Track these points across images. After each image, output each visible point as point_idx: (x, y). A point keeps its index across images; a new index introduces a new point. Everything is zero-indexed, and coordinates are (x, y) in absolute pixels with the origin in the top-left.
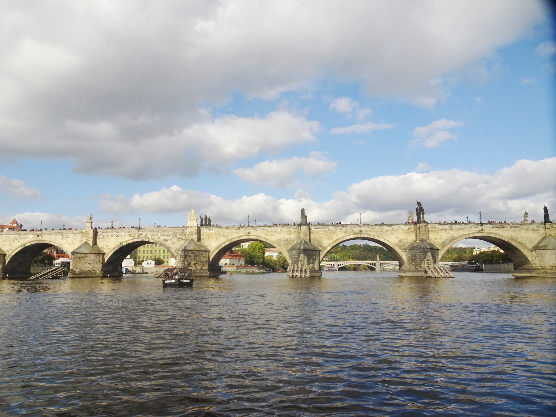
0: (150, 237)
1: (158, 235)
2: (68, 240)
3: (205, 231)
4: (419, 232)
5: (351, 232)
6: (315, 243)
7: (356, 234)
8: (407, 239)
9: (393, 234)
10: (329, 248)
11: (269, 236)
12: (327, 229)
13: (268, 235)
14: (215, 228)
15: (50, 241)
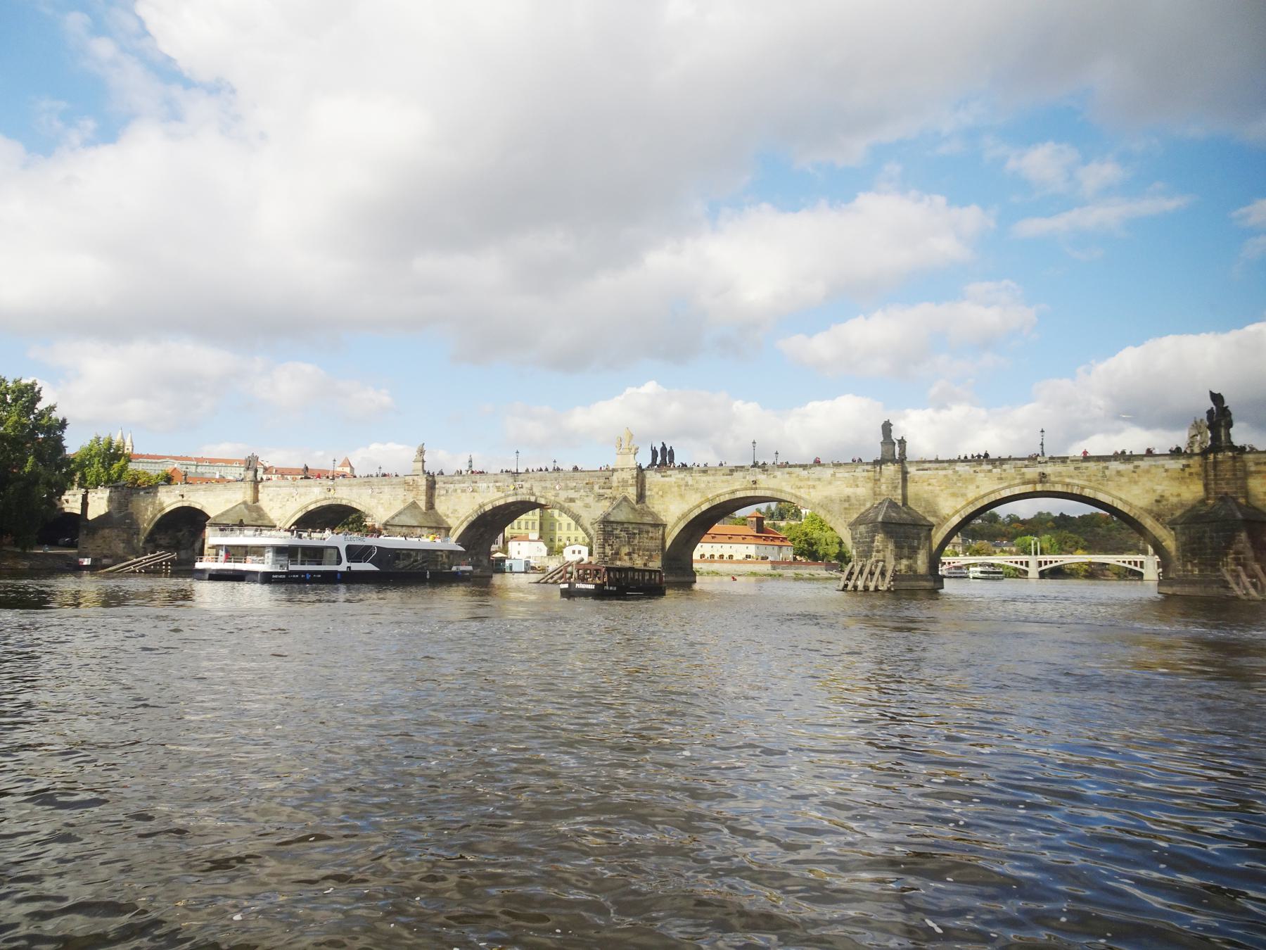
0: (538, 494)
1: (554, 489)
2: (382, 499)
3: (655, 479)
4: (1215, 475)
5: (1015, 479)
6: (920, 506)
7: (1028, 483)
8: (1179, 495)
9: (1136, 482)
10: (956, 520)
11: (802, 490)
12: (950, 472)
13: (800, 487)
14: (677, 471)
15: (350, 501)
